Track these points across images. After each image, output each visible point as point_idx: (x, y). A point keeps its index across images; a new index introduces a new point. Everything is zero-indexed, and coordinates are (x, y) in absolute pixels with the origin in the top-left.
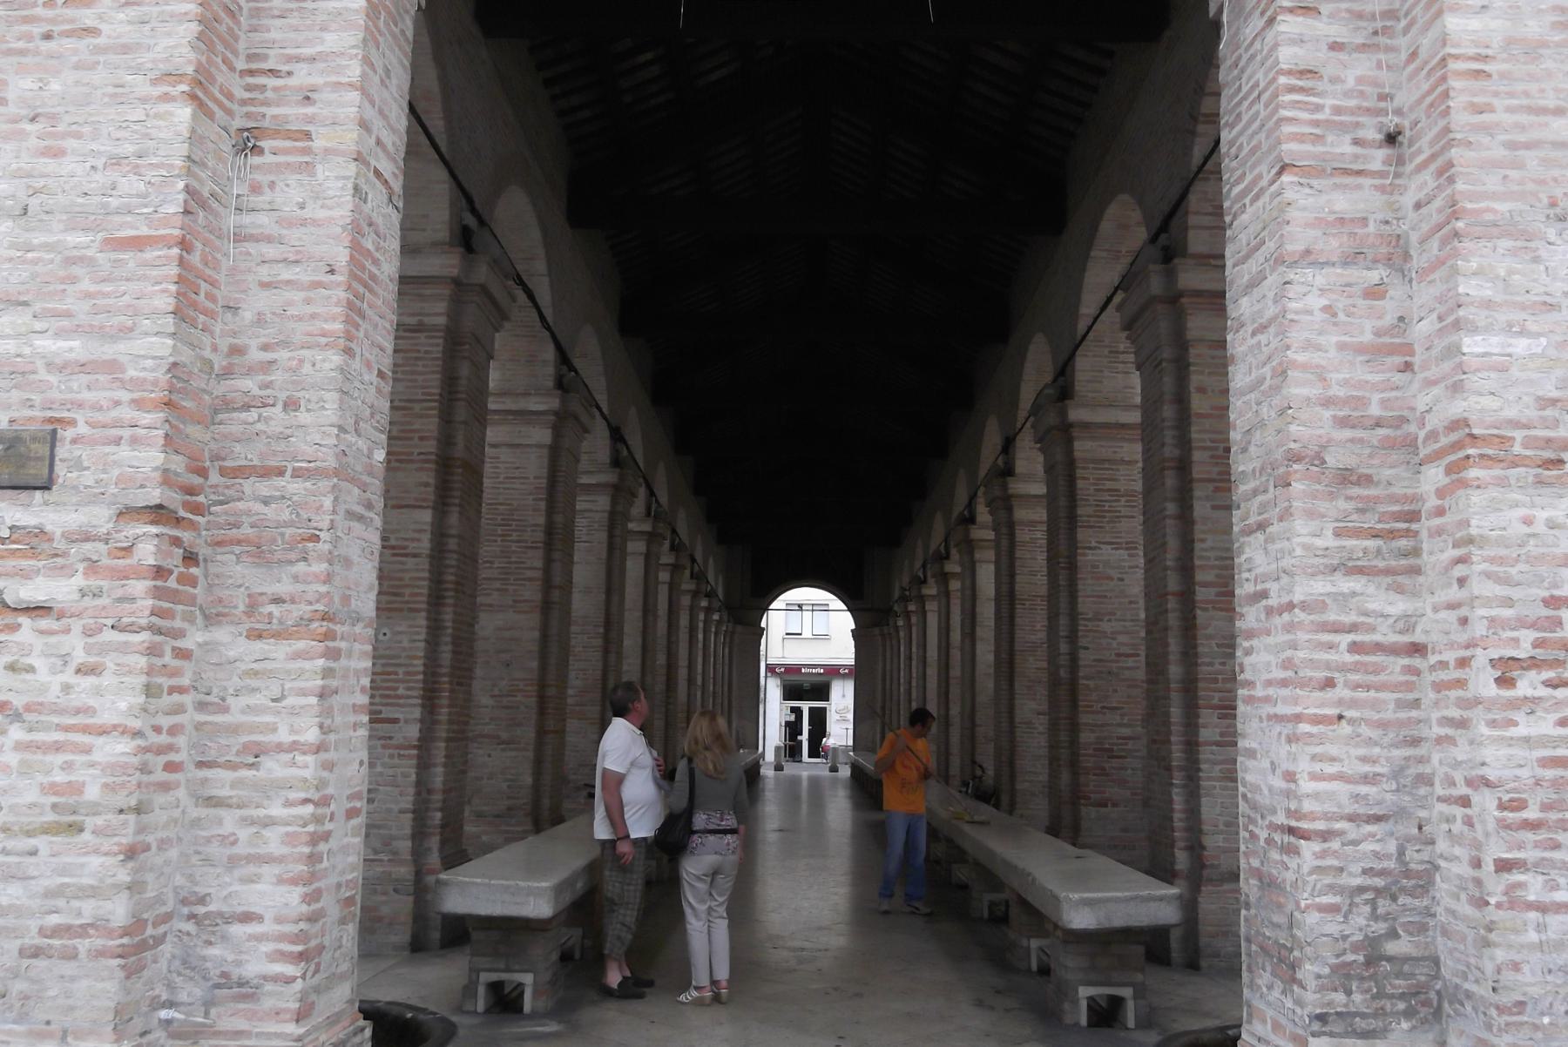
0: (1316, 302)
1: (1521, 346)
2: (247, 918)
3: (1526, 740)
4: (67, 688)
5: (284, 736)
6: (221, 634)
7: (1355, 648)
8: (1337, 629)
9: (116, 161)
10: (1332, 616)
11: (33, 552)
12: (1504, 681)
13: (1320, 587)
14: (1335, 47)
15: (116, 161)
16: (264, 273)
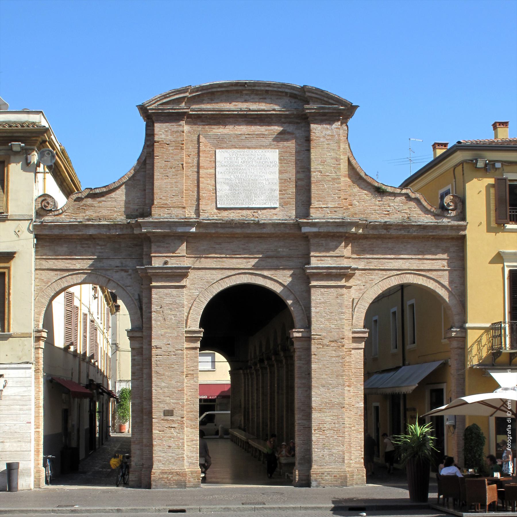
0: (300, 392)
1: (317, 399)
2: (193, 457)
3: (316, 437)
4: (177, 435)
5: (195, 439)
6: (188, 429)
7: (303, 428)
8: (301, 426)
9: (177, 382)
10: (301, 424)
11: (172, 422)
12: (314, 431)
13: (300, 422)
14: (303, 364)
15: (177, 382)
16: (190, 390)
